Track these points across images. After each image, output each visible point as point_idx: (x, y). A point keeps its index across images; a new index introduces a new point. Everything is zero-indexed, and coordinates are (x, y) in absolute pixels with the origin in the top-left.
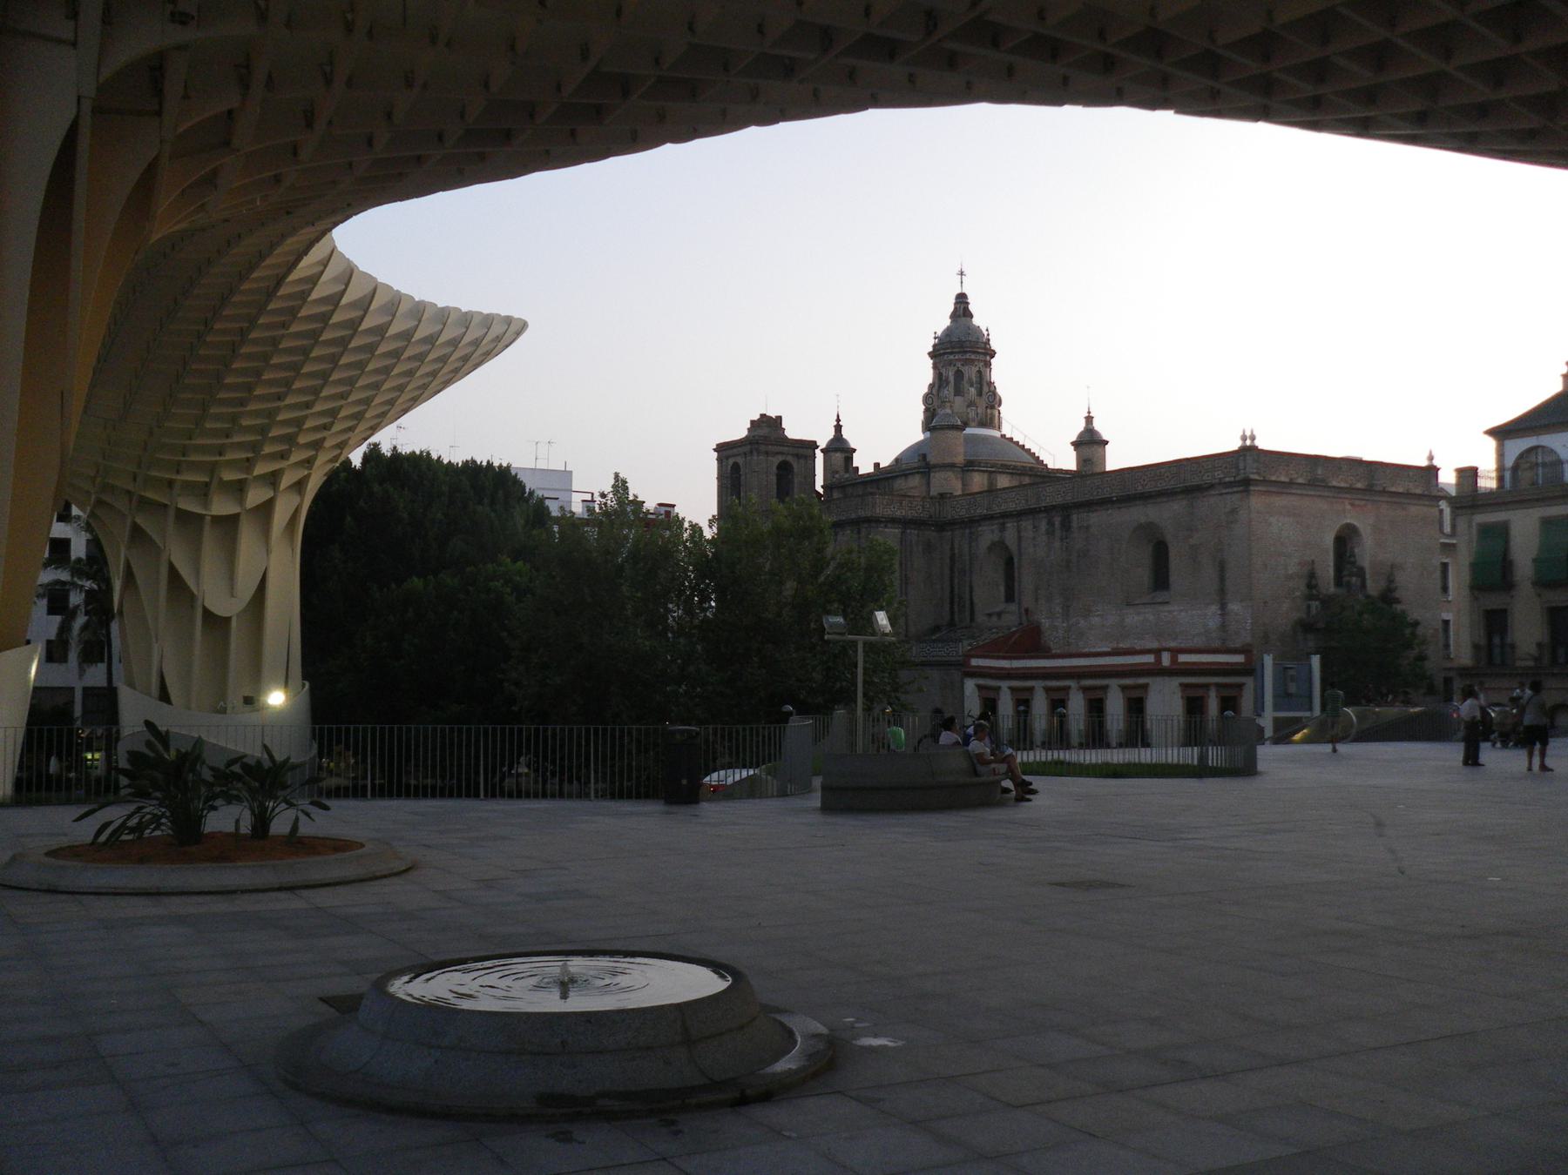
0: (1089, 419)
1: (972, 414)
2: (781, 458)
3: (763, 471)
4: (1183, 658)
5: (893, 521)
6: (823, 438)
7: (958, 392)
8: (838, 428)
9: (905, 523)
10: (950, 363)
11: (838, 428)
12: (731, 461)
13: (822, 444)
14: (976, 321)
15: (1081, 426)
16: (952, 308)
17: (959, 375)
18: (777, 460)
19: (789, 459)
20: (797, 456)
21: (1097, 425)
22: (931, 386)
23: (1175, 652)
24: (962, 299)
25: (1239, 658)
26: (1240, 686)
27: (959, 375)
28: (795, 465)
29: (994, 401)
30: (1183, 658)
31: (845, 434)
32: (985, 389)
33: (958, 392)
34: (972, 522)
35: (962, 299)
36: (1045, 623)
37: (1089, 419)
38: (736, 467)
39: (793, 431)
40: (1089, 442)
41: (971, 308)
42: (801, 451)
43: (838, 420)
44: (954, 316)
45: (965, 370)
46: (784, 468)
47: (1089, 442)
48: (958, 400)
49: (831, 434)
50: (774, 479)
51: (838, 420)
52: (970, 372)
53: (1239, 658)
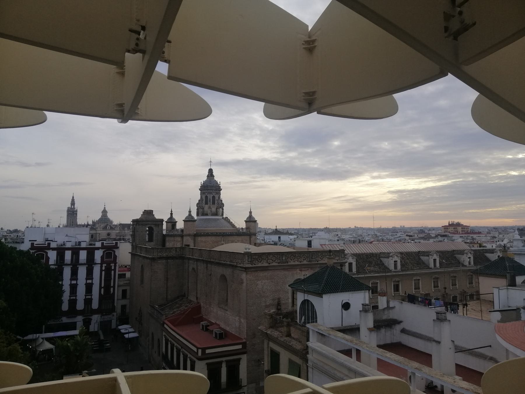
0: (251, 212)
1: (209, 212)
4: (208, 351)
5: (161, 258)
6: (166, 218)
7: (206, 203)
8: (171, 214)
9: (167, 258)
10: (204, 193)
11: (171, 214)
13: (166, 219)
14: (215, 178)
15: (248, 215)
16: (207, 173)
17: (206, 197)
19: (153, 226)
20: (155, 225)
21: (253, 215)
22: (199, 201)
23: (204, 350)
24: (211, 171)
25: (240, 347)
26: (239, 360)
27: (206, 197)
28: (155, 229)
29: (221, 205)
30: (208, 351)
31: (174, 216)
32: (216, 202)
33: (206, 203)
34: (189, 259)
35: (211, 171)
36: (202, 304)
37: (251, 212)
39: (157, 216)
40: (251, 220)
41: (214, 174)
42: (157, 223)
43: (172, 211)
44: (208, 176)
45: (208, 196)
46: (151, 230)
47: (251, 220)
48: (206, 206)
49: (169, 216)
51: (172, 211)
52: (210, 197)
53: (240, 347)
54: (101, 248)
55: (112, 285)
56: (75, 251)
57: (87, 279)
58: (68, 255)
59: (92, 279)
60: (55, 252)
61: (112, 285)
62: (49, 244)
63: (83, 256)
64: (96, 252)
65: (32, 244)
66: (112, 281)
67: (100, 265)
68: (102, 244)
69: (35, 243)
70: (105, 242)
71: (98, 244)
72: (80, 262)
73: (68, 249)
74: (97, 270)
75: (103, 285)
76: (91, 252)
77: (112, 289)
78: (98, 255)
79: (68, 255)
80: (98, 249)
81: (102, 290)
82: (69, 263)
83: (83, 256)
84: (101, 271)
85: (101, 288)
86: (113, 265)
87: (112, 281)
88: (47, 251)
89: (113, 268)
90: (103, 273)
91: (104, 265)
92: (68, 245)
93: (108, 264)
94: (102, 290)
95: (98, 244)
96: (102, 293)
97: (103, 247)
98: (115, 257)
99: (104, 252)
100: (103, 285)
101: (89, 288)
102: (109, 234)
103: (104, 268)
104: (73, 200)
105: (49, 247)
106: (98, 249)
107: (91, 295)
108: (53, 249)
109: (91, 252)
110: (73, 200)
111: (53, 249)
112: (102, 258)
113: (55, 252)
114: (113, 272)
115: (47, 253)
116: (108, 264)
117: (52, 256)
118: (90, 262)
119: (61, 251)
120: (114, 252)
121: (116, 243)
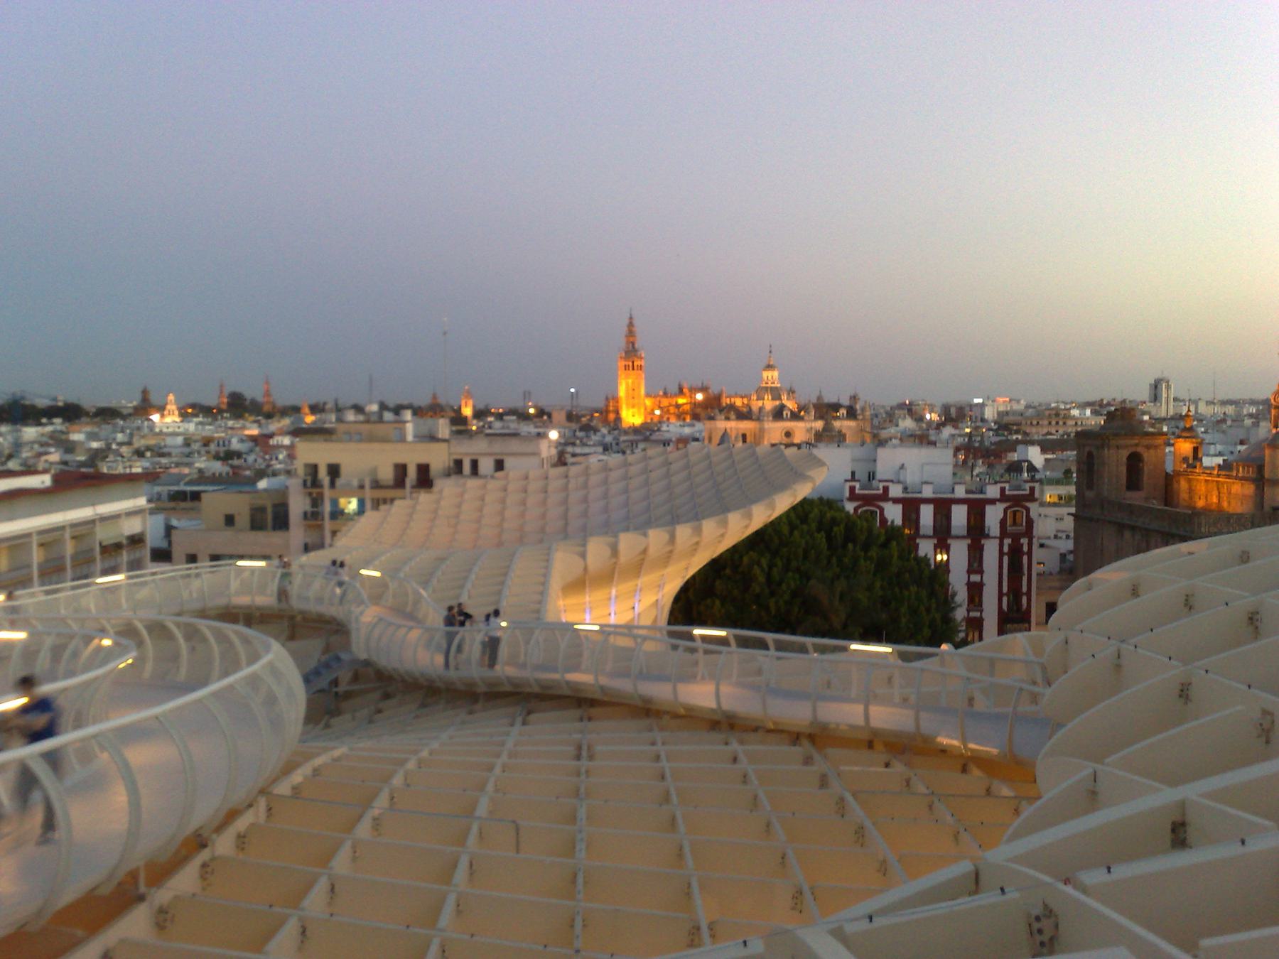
2: (1133, 450)
3: (1115, 460)
12: (1087, 449)
18: (1125, 454)
19: (1139, 449)
28: (1148, 456)
38: (1090, 455)
50: (1124, 469)
54: (1001, 500)
55: (1025, 589)
56: (943, 507)
57: (969, 572)
58: (927, 513)
59: (981, 572)
60: (899, 508)
61: (1025, 589)
62: (886, 489)
63: (959, 516)
64: (989, 510)
65: (852, 489)
66: (1025, 579)
67: (997, 541)
68: (1003, 490)
69: (857, 485)
70: (1007, 486)
71: (993, 491)
72: (954, 532)
73: (927, 501)
74: (991, 550)
75: (1005, 589)
76: (977, 509)
77: (1024, 599)
78: (993, 516)
79: (927, 513)
80: (992, 502)
81: (1005, 599)
82: (931, 533)
83: (959, 516)
84: (1001, 554)
85: (1001, 595)
86: (1024, 541)
87: (1025, 579)
88: (882, 504)
89: (1025, 549)
90: (1006, 559)
91: (1007, 541)
92: (928, 492)
93: (1016, 538)
94: (1005, 599)
95: (993, 491)
96: (1005, 607)
97: (1003, 497)
98: (1030, 523)
99: (1005, 511)
100: (1005, 589)
101: (975, 591)
102: (788, 434)
103: (1006, 549)
104: (631, 325)
105: (885, 496)
106: (992, 502)
107: (981, 611)
108: (896, 501)
109: (977, 509)
110: (631, 325)
111: (896, 501)
112: (1003, 523)
113: (899, 508)
114: (1025, 558)
115: (882, 510)
116: (1016, 538)
117: (894, 513)
118: (976, 531)
119: (911, 506)
120: (1028, 510)
121: (1032, 489)
